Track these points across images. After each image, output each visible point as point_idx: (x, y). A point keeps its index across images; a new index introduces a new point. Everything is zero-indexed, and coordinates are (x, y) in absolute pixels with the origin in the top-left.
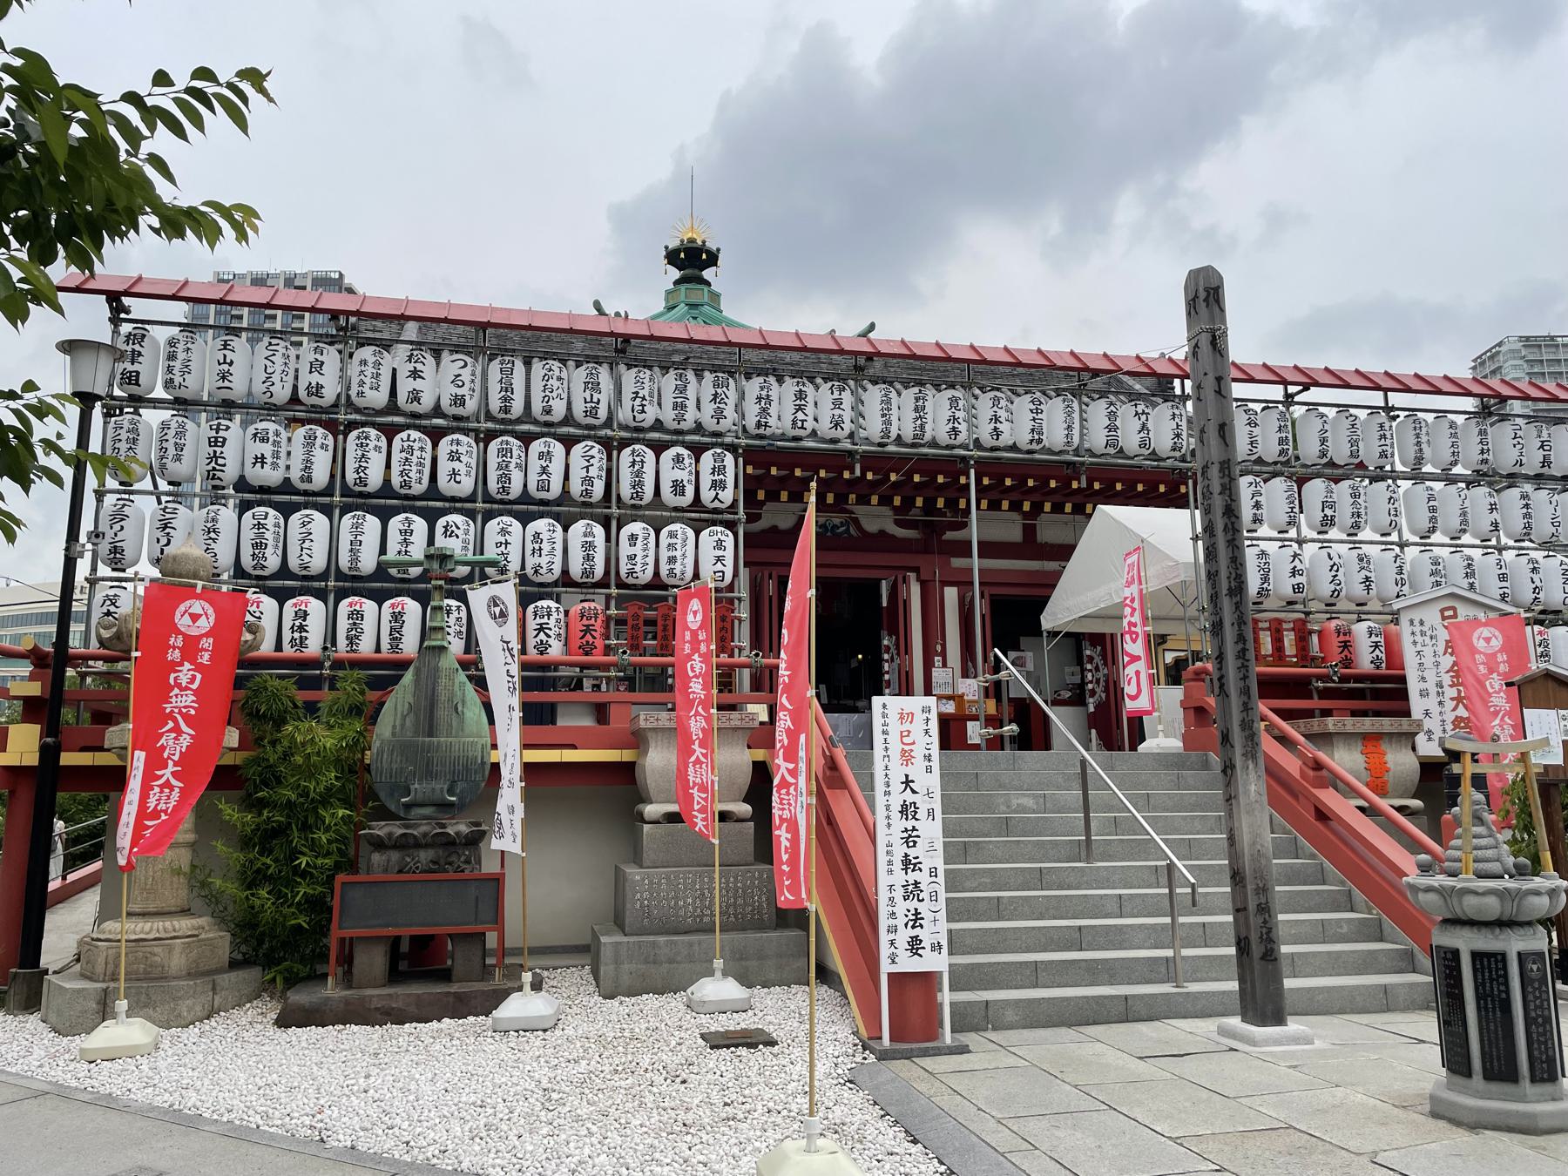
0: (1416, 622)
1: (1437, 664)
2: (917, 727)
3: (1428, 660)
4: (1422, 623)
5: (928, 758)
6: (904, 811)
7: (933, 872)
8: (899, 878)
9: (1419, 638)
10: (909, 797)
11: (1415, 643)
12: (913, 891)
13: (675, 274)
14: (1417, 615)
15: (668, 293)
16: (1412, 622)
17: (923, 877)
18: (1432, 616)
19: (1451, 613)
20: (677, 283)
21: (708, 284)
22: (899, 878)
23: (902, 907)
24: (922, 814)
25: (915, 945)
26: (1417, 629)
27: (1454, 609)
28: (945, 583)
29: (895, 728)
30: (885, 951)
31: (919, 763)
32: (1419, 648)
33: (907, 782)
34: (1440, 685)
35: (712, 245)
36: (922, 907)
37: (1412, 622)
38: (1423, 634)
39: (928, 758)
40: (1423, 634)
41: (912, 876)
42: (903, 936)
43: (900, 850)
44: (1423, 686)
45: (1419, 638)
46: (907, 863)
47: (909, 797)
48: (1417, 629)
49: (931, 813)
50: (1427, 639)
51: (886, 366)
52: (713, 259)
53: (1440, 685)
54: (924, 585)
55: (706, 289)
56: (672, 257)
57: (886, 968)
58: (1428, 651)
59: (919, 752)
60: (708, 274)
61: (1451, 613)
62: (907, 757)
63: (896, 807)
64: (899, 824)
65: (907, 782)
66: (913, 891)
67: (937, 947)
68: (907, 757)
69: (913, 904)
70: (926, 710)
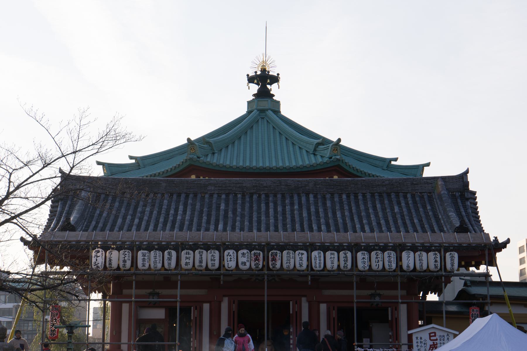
0: (419, 338)
4: (421, 338)
9: (419, 344)
11: (418, 346)
13: (255, 88)
14: (419, 335)
15: (249, 103)
16: (417, 338)
19: (433, 334)
20: (254, 95)
21: (273, 95)
26: (419, 341)
27: (435, 333)
28: (319, 302)
32: (419, 348)
37: (417, 338)
38: (421, 342)
45: (419, 344)
48: (419, 341)
50: (423, 345)
52: (275, 79)
54: (309, 302)
55: (269, 100)
56: (251, 80)
60: (273, 88)
61: (433, 334)
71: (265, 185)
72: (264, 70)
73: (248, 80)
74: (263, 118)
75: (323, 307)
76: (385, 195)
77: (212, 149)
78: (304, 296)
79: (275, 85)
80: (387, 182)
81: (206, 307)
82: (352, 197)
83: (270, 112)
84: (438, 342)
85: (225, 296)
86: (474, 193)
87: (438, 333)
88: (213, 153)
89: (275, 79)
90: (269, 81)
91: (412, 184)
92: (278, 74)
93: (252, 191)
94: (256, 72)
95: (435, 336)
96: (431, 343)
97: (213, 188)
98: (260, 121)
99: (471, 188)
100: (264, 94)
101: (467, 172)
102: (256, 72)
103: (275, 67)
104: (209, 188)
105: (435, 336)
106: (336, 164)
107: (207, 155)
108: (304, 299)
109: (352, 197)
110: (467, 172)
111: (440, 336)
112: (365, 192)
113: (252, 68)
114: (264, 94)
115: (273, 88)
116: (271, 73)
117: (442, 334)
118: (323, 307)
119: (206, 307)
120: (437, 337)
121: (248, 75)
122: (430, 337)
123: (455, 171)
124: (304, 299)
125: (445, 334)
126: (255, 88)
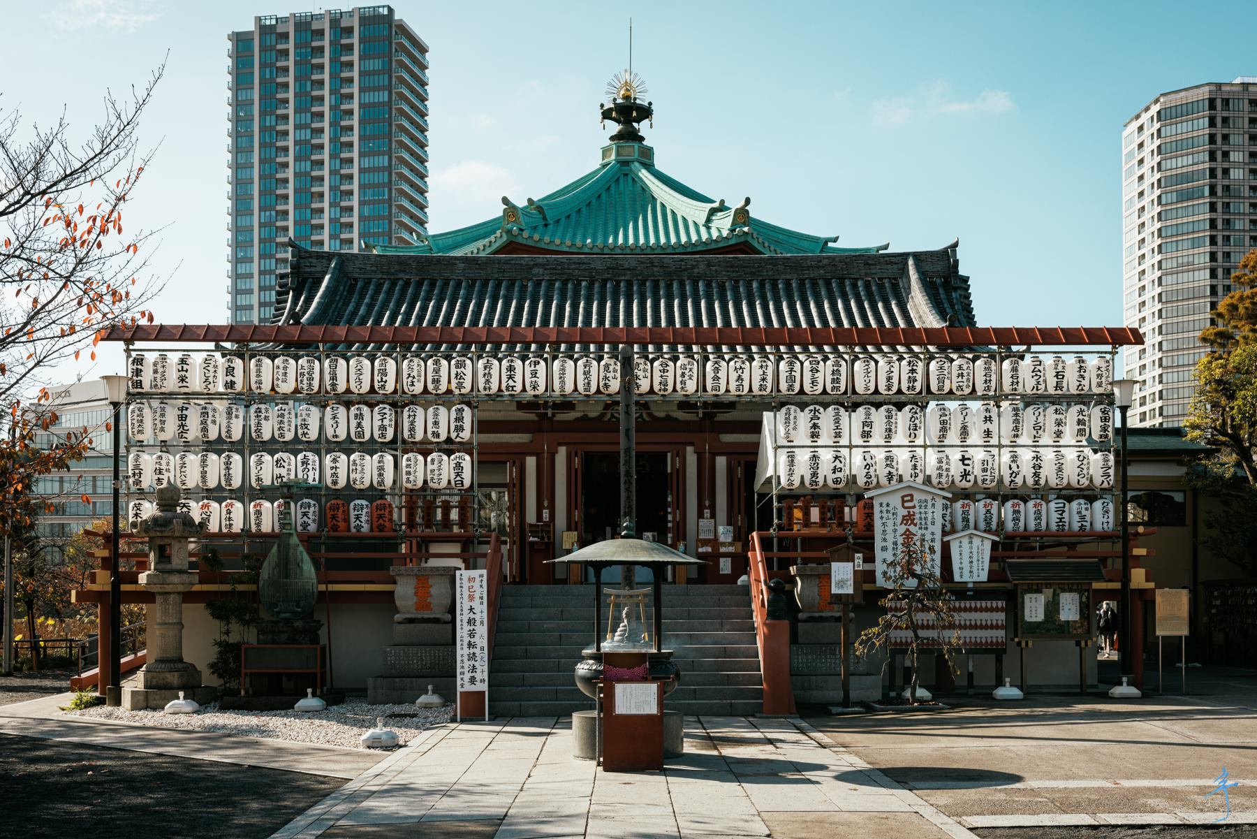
1: (895, 531)
2: (477, 584)
3: (890, 529)
4: (888, 505)
5: (481, 598)
6: (469, 622)
7: (482, 648)
8: (466, 651)
9: (885, 515)
10: (472, 616)
12: (472, 657)
13: (614, 128)
16: (881, 505)
17: (477, 651)
18: (895, 501)
20: (612, 138)
21: (642, 139)
22: (466, 651)
23: (467, 664)
24: (478, 623)
25: (473, 680)
26: (884, 509)
27: (911, 496)
28: (714, 455)
29: (466, 584)
30: (459, 682)
31: (477, 600)
33: (471, 609)
34: (895, 543)
35: (643, 100)
36: (477, 664)
37: (881, 505)
38: (888, 512)
39: (481, 598)
40: (888, 512)
41: (472, 651)
42: (467, 676)
43: (467, 639)
44: (884, 544)
45: (885, 515)
46: (470, 645)
47: (472, 616)
49: (482, 623)
51: (709, 265)
52: (646, 112)
53: (895, 543)
55: (636, 145)
56: (606, 115)
57: (459, 689)
58: (890, 523)
59: (477, 595)
60: (643, 127)
62: (471, 598)
63: (465, 621)
64: (467, 628)
65: (471, 609)
66: (472, 657)
67: (482, 681)
68: (471, 598)
69: (472, 663)
70: (481, 576)
71: (626, 266)
72: (627, 98)
73: (603, 113)
74: (626, 175)
75: (721, 462)
76: (821, 282)
77: (545, 218)
78: (692, 444)
79: (645, 123)
80: (826, 262)
81: (531, 462)
82: (768, 287)
83: (637, 164)
84: (917, 510)
85: (560, 444)
86: (965, 280)
87: (917, 496)
88: (546, 225)
89: (646, 112)
90: (634, 114)
91: (866, 264)
92: (650, 104)
93: (606, 276)
94: (615, 99)
95: (912, 500)
96: (905, 512)
97: (541, 271)
98: (622, 179)
99: (962, 271)
100: (629, 136)
101: (956, 245)
102: (615, 99)
103: (645, 91)
104: (536, 270)
105: (912, 500)
106: (742, 239)
107: (535, 228)
108: (690, 449)
109: (768, 287)
110: (956, 245)
111: (920, 501)
112: (788, 277)
113: (608, 93)
114: (629, 136)
115: (643, 127)
116: (638, 101)
117: (923, 497)
118: (721, 462)
119: (531, 462)
120: (915, 502)
121: (602, 106)
122: (903, 502)
123: (935, 244)
124: (690, 449)
125: (929, 498)
126: (614, 128)
